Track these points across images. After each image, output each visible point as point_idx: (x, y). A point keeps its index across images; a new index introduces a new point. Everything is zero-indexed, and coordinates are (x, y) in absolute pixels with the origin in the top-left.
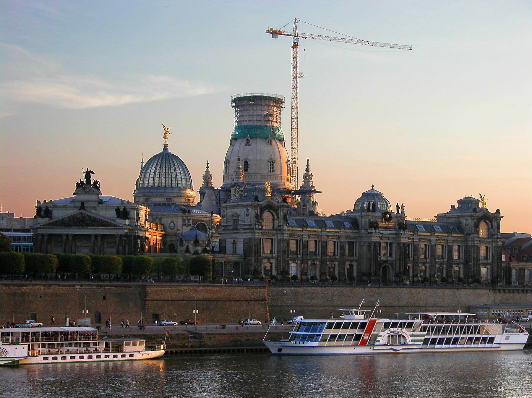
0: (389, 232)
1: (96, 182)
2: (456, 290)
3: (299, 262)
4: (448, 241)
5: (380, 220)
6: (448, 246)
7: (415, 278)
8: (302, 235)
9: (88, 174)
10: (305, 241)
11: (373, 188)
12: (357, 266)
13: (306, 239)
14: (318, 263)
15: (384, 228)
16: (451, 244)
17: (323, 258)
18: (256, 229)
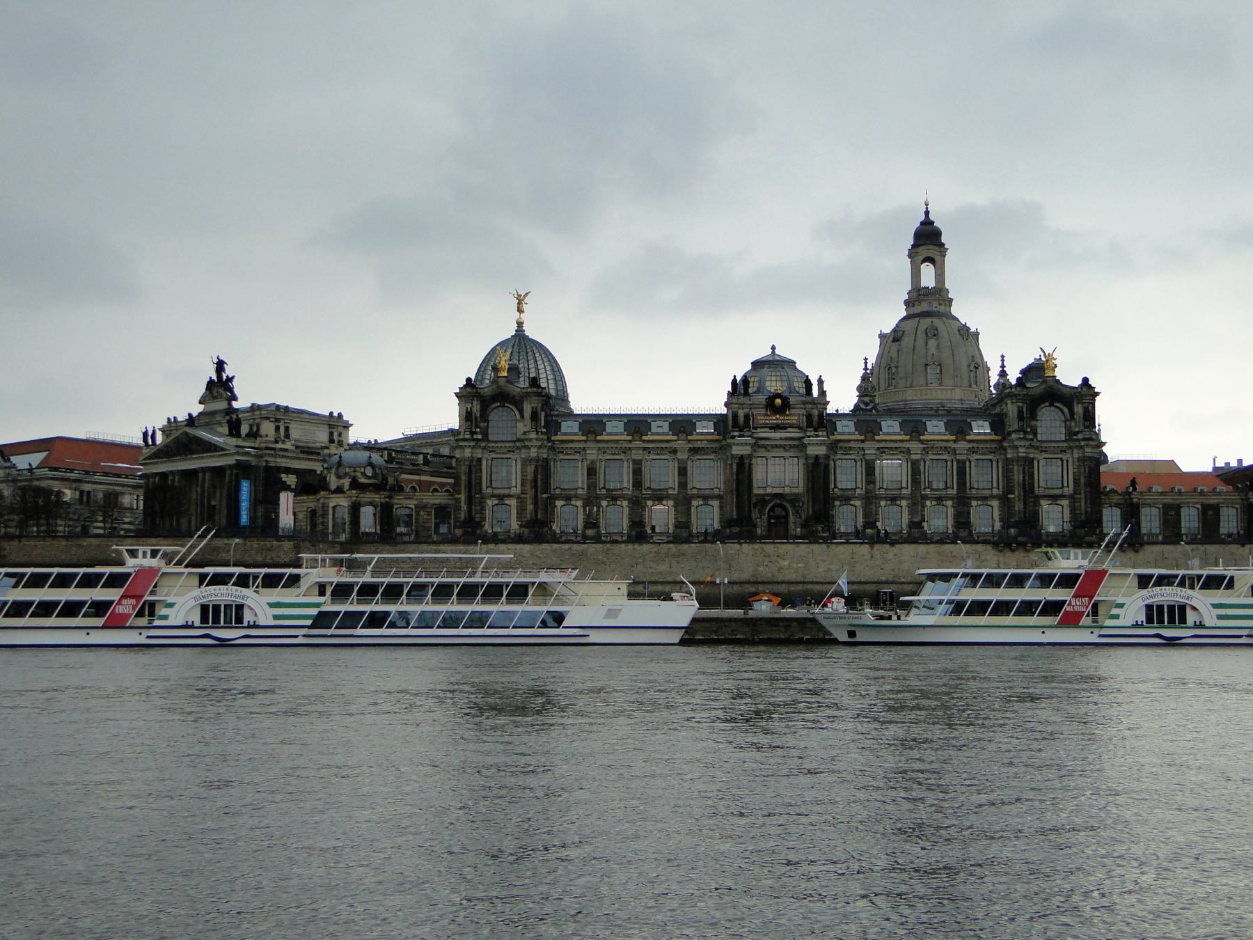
0: (784, 435)
1: (230, 379)
2: (887, 546)
3: (579, 503)
4: (955, 450)
5: (763, 411)
6: (958, 461)
7: (869, 531)
8: (584, 449)
9: (220, 366)
10: (593, 462)
11: (773, 352)
12: (721, 507)
13: (594, 457)
14: (625, 503)
15: (771, 428)
16: (964, 457)
17: (637, 493)
18: (465, 440)
